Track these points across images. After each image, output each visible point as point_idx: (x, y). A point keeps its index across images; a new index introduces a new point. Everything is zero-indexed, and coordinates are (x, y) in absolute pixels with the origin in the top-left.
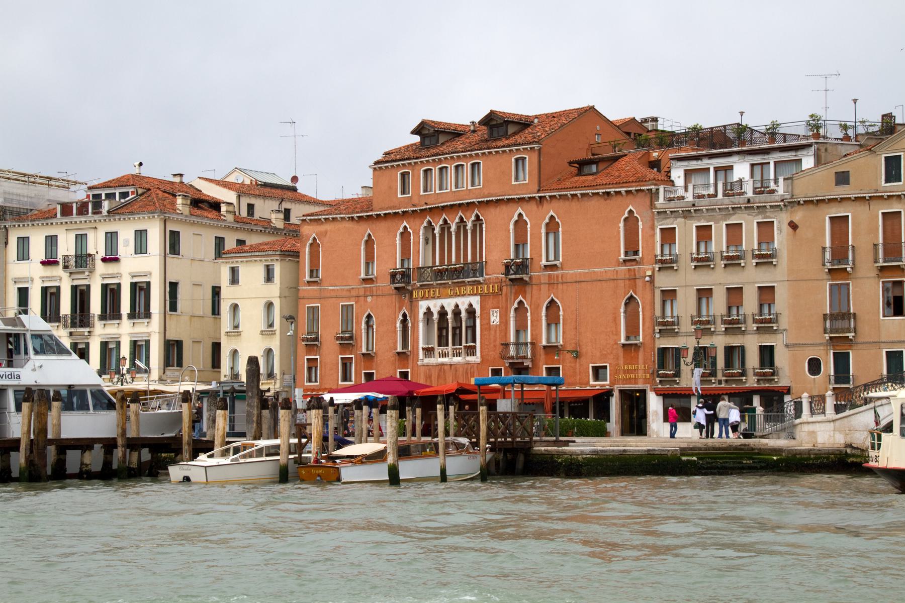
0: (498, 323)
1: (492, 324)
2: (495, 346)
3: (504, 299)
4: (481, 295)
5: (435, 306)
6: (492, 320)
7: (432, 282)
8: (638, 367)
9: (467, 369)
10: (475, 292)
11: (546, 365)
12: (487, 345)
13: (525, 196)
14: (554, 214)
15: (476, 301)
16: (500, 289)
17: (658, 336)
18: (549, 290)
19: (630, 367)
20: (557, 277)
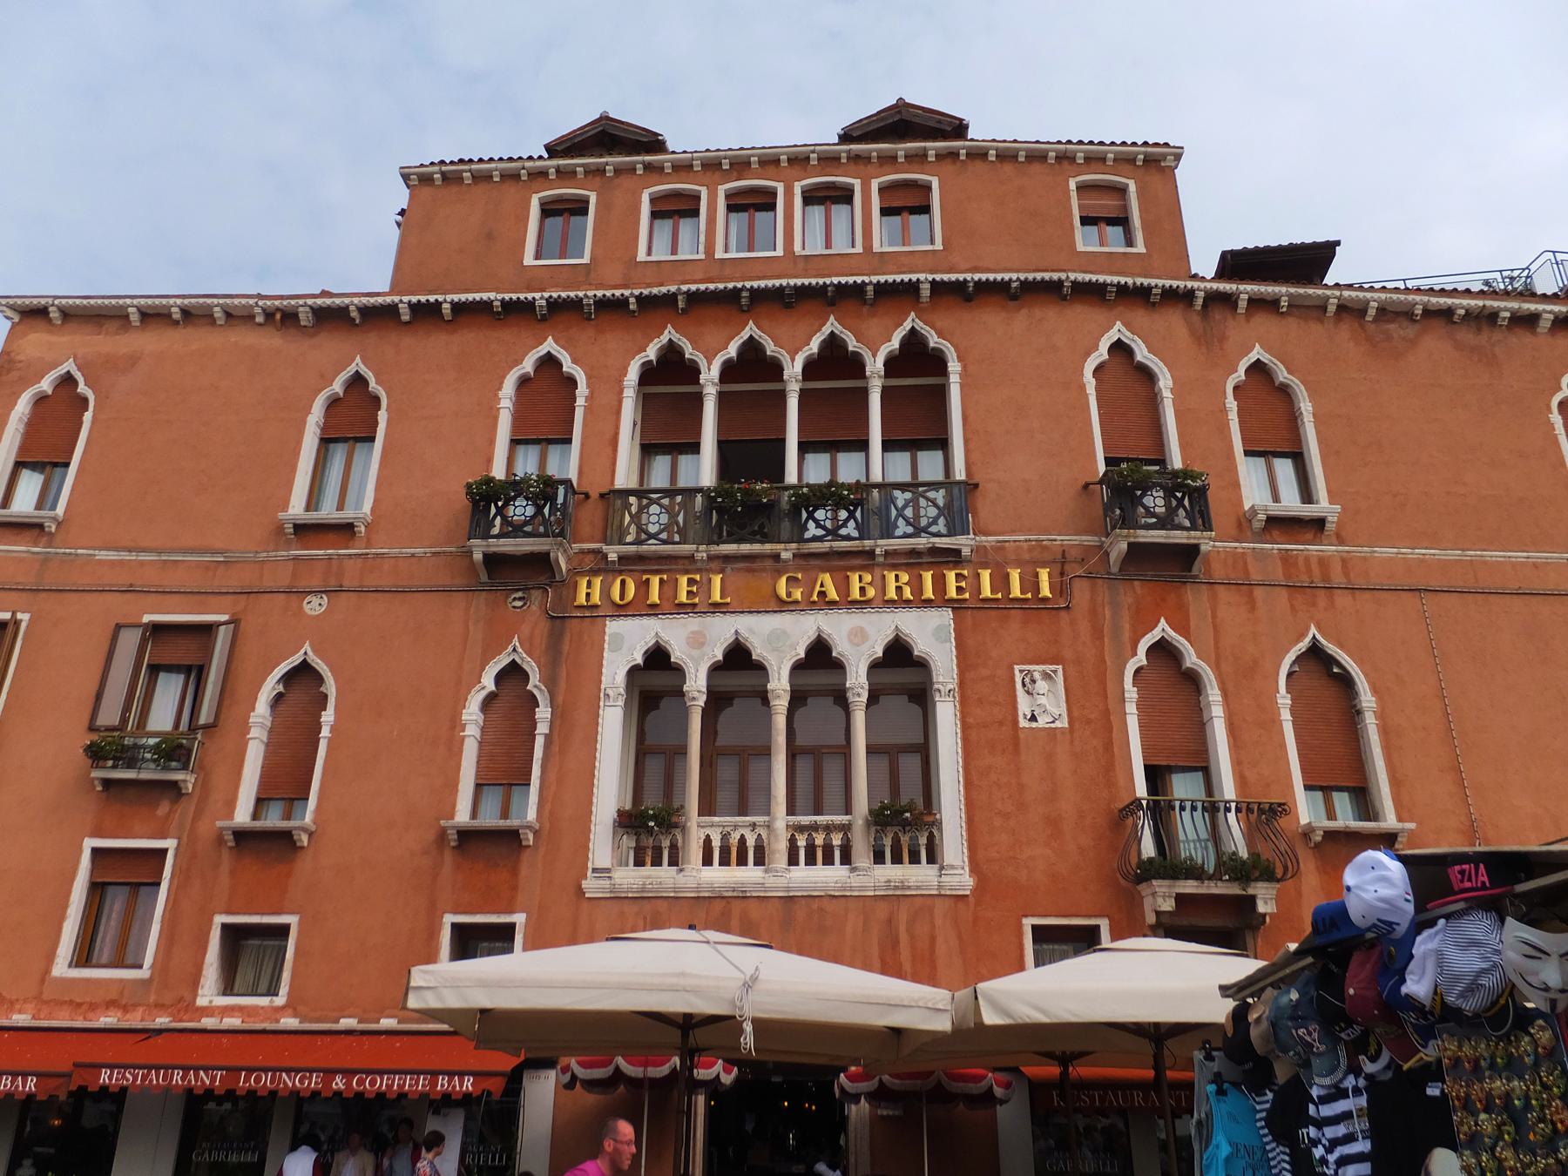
0: (1063, 723)
1: (1023, 723)
2: (1053, 823)
3: (1084, 627)
4: (957, 606)
5: (697, 641)
6: (1024, 705)
7: (688, 548)
9: (890, 921)
10: (929, 593)
12: (1006, 816)
13: (1153, 282)
16: (1060, 588)
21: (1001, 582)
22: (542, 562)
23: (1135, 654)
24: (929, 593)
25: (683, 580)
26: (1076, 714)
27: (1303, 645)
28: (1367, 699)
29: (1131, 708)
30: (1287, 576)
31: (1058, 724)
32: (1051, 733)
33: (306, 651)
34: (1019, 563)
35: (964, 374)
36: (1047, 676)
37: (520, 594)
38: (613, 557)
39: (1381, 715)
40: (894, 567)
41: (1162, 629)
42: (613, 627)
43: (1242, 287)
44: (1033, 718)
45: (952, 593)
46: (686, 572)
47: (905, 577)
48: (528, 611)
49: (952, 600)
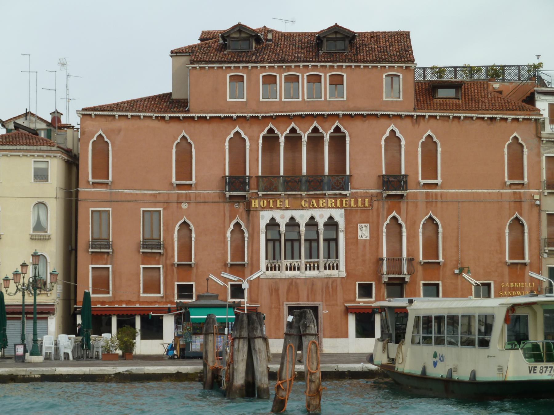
0: (368, 238)
1: (359, 238)
2: (364, 261)
3: (375, 214)
8: (524, 285)
11: (424, 280)
14: (431, 134)
15: (339, 216)
16: (371, 204)
17: (545, 256)
18: (427, 207)
19: (516, 285)
20: (436, 194)
31: (367, 238)
43: (426, 114)
44: (362, 237)
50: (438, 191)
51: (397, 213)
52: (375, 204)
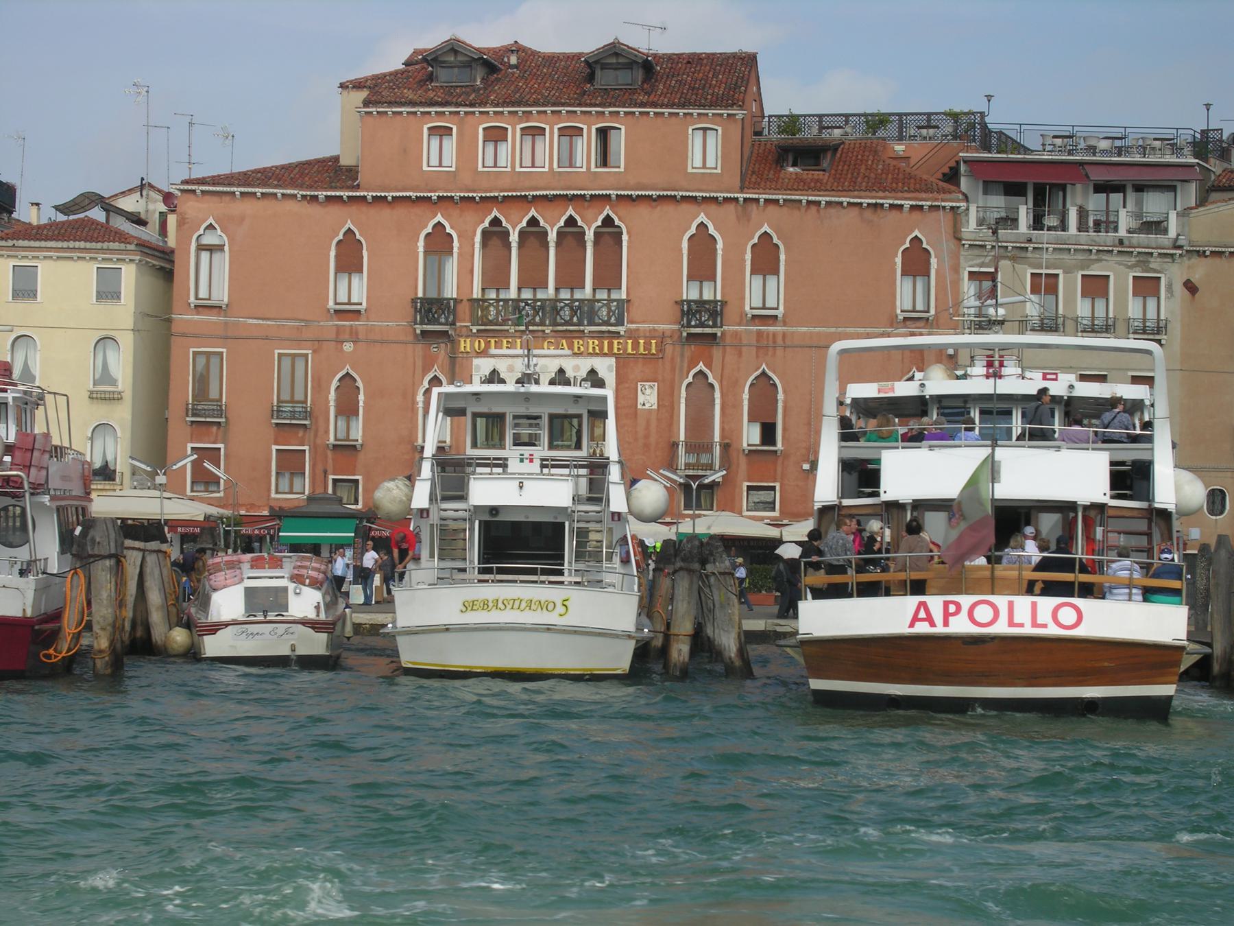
0: (655, 407)
1: (639, 407)
4: (617, 357)
5: (511, 369)
6: (641, 399)
10: (606, 350)
15: (606, 367)
16: (661, 348)
18: (757, 357)
20: (774, 334)
21: (636, 346)
22: (445, 334)
23: (687, 377)
24: (606, 350)
25: (505, 341)
26: (661, 403)
27: (758, 373)
28: (781, 396)
29: (683, 401)
30: (758, 341)
31: (653, 407)
32: (650, 411)
33: (348, 368)
34: (645, 337)
35: (629, 241)
36: (651, 387)
37: (435, 346)
38: (474, 331)
39: (785, 402)
40: (593, 338)
41: (701, 366)
42: (476, 361)
44: (644, 405)
45: (615, 351)
46: (506, 337)
47: (596, 342)
48: (440, 351)
49: (615, 354)
50: (778, 329)
51: (706, 367)
52: (669, 349)
